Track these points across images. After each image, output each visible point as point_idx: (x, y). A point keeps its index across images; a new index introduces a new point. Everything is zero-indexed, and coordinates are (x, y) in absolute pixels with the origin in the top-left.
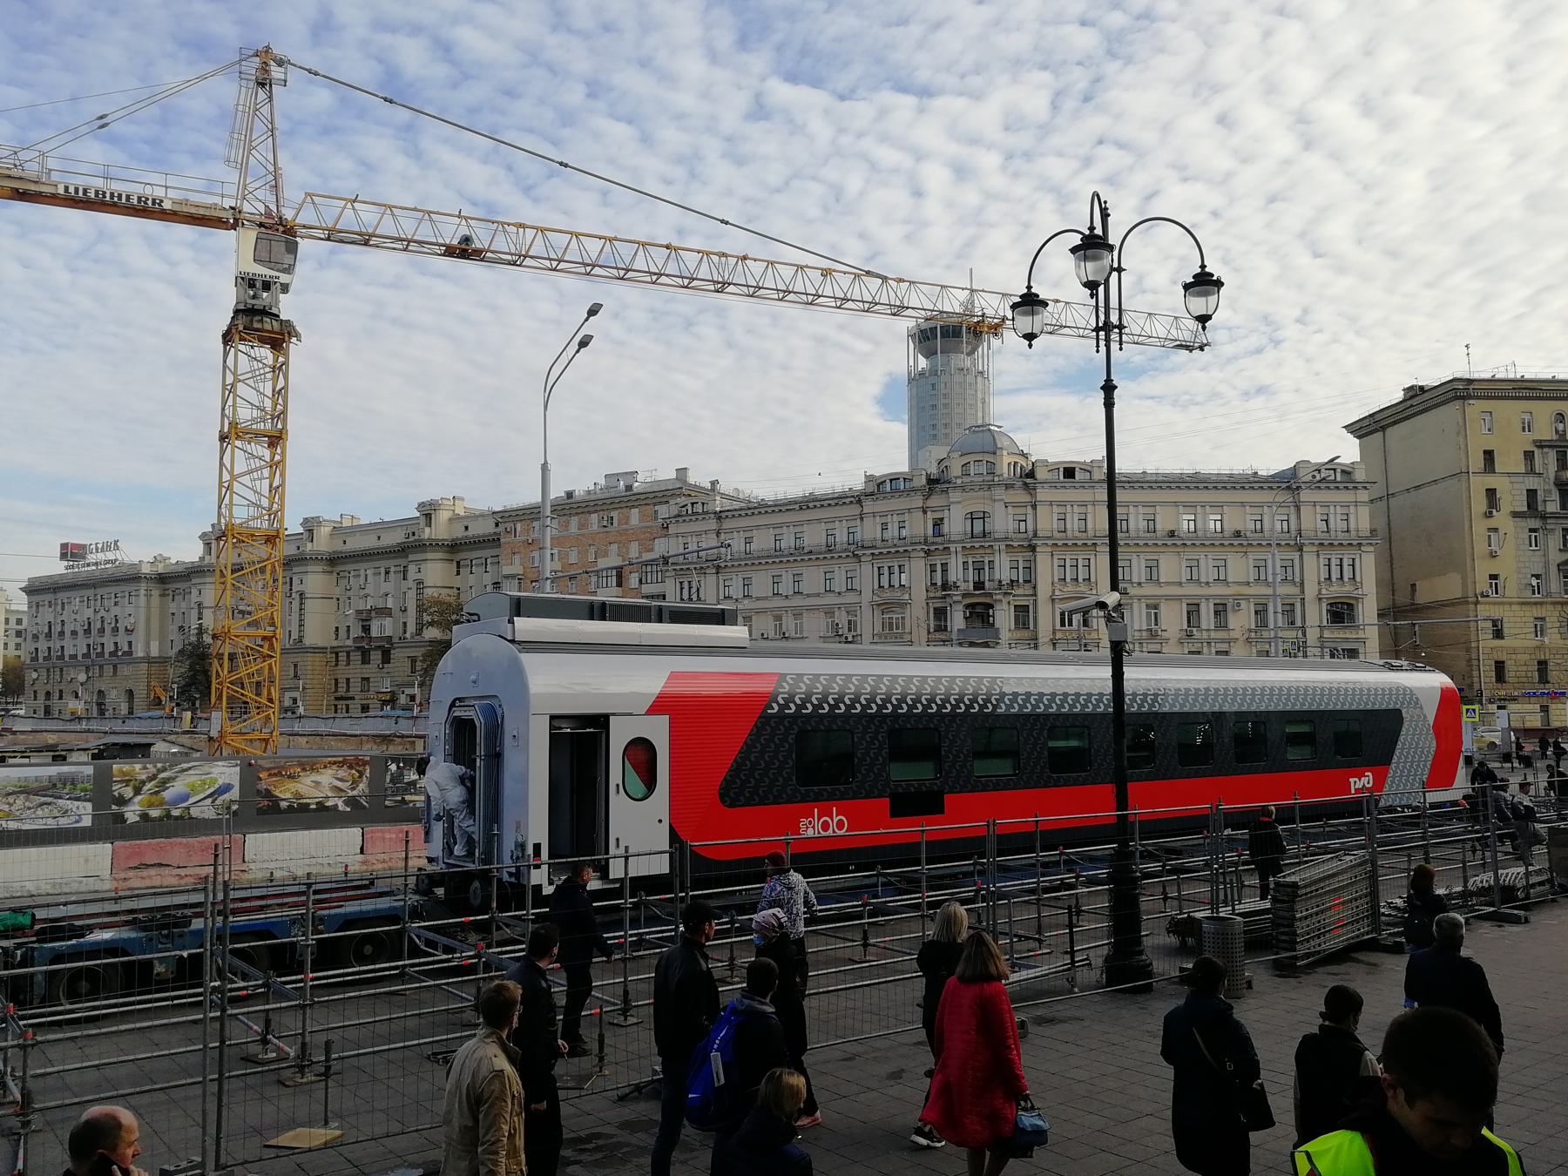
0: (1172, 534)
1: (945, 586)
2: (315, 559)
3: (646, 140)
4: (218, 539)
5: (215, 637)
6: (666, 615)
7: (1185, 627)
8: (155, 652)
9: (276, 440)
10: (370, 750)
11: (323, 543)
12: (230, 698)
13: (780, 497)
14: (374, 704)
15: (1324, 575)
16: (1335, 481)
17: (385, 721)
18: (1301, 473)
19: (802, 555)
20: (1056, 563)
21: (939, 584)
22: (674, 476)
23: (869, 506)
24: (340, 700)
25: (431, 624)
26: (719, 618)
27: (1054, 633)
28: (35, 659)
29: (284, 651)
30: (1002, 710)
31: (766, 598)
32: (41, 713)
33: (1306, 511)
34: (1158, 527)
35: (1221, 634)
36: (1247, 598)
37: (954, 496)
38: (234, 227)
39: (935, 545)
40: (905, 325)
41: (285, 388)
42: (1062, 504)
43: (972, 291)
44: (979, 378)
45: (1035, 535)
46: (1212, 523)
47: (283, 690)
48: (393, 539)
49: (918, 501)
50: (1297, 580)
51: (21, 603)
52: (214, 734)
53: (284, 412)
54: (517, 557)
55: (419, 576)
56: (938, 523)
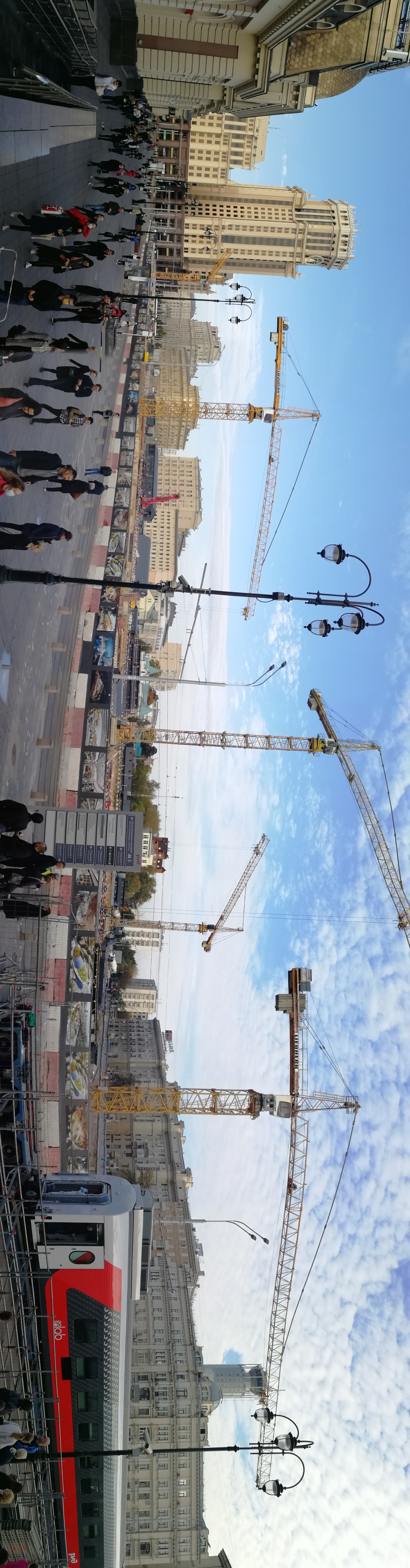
0: (178, 1475)
1: (156, 1380)
2: (168, 1126)
3: (334, 1259)
4: (175, 1089)
5: (137, 1088)
6: (145, 1268)
7: (140, 1481)
8: (132, 1065)
9: (213, 1110)
10: (91, 1149)
11: (174, 1129)
12: (113, 1094)
13: (193, 1312)
14: (110, 1150)
15: (161, 1541)
16: (200, 1545)
17: (103, 1155)
18: (204, 1531)
19: (170, 1320)
20: (166, 1426)
21: (158, 1378)
22: (201, 1270)
23: (189, 1348)
24: (111, 1137)
25: (142, 1174)
26: (143, 1288)
27: (138, 1425)
28: (130, 1022)
29: (131, 1115)
30: (105, 1404)
31: (152, 1306)
32: (110, 1024)
33: (188, 1533)
34: (181, 1469)
35: (136, 1497)
36: (152, 1508)
37: (194, 1384)
38: (291, 1094)
39: (173, 1376)
40: (262, 1362)
41: (234, 1114)
42: (190, 1428)
43: (278, 1391)
44: (241, 1394)
45: (178, 1417)
46: (183, 1493)
47: (116, 1114)
48: (176, 1159)
49: (191, 1368)
50: (159, 1529)
51: (151, 1017)
52: (99, 1088)
53: (224, 1114)
54: (169, 1208)
55: (161, 1168)
56: (182, 1377)
